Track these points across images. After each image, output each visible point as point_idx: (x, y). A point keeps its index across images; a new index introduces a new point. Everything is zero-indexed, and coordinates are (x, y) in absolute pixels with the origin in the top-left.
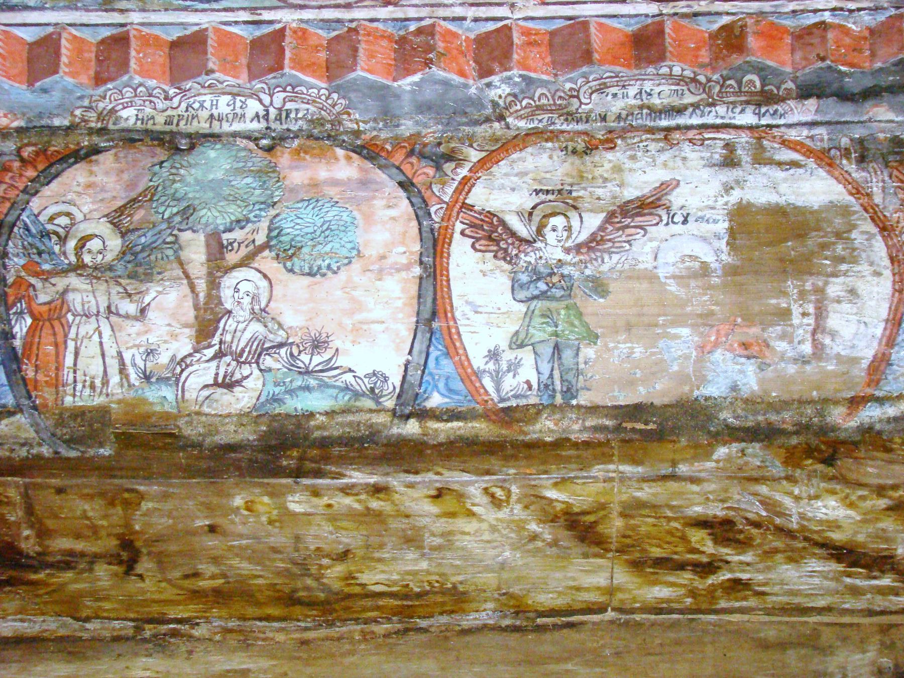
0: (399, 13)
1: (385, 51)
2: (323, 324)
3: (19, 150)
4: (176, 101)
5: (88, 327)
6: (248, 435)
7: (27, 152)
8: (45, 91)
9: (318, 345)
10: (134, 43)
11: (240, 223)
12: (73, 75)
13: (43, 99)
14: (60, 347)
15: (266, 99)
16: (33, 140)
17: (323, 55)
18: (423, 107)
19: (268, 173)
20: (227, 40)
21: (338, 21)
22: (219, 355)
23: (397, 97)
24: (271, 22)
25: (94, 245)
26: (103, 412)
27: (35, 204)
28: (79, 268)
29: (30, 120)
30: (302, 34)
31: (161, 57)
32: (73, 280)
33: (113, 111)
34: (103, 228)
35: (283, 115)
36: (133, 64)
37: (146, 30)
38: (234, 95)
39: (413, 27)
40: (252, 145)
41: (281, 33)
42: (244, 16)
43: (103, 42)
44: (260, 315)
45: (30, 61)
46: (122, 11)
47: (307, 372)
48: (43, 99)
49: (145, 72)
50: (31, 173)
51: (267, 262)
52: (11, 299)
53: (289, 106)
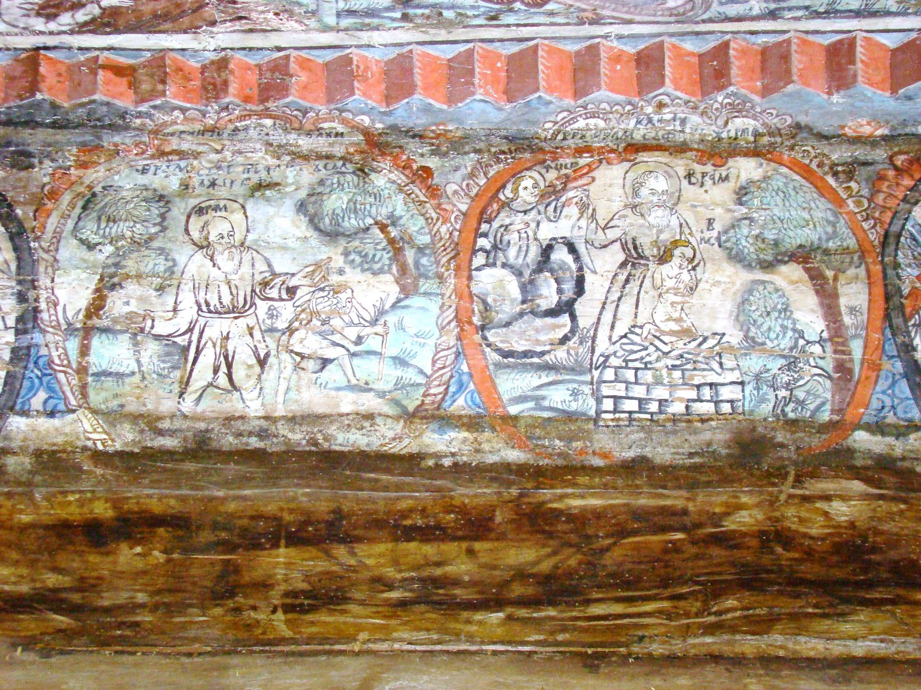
3: (891, 158)
7: (900, 160)
8: (909, 98)
13: (907, 106)
16: (904, 148)
29: (893, 128)
45: (893, 67)
50: (907, 182)
52: (908, 310)
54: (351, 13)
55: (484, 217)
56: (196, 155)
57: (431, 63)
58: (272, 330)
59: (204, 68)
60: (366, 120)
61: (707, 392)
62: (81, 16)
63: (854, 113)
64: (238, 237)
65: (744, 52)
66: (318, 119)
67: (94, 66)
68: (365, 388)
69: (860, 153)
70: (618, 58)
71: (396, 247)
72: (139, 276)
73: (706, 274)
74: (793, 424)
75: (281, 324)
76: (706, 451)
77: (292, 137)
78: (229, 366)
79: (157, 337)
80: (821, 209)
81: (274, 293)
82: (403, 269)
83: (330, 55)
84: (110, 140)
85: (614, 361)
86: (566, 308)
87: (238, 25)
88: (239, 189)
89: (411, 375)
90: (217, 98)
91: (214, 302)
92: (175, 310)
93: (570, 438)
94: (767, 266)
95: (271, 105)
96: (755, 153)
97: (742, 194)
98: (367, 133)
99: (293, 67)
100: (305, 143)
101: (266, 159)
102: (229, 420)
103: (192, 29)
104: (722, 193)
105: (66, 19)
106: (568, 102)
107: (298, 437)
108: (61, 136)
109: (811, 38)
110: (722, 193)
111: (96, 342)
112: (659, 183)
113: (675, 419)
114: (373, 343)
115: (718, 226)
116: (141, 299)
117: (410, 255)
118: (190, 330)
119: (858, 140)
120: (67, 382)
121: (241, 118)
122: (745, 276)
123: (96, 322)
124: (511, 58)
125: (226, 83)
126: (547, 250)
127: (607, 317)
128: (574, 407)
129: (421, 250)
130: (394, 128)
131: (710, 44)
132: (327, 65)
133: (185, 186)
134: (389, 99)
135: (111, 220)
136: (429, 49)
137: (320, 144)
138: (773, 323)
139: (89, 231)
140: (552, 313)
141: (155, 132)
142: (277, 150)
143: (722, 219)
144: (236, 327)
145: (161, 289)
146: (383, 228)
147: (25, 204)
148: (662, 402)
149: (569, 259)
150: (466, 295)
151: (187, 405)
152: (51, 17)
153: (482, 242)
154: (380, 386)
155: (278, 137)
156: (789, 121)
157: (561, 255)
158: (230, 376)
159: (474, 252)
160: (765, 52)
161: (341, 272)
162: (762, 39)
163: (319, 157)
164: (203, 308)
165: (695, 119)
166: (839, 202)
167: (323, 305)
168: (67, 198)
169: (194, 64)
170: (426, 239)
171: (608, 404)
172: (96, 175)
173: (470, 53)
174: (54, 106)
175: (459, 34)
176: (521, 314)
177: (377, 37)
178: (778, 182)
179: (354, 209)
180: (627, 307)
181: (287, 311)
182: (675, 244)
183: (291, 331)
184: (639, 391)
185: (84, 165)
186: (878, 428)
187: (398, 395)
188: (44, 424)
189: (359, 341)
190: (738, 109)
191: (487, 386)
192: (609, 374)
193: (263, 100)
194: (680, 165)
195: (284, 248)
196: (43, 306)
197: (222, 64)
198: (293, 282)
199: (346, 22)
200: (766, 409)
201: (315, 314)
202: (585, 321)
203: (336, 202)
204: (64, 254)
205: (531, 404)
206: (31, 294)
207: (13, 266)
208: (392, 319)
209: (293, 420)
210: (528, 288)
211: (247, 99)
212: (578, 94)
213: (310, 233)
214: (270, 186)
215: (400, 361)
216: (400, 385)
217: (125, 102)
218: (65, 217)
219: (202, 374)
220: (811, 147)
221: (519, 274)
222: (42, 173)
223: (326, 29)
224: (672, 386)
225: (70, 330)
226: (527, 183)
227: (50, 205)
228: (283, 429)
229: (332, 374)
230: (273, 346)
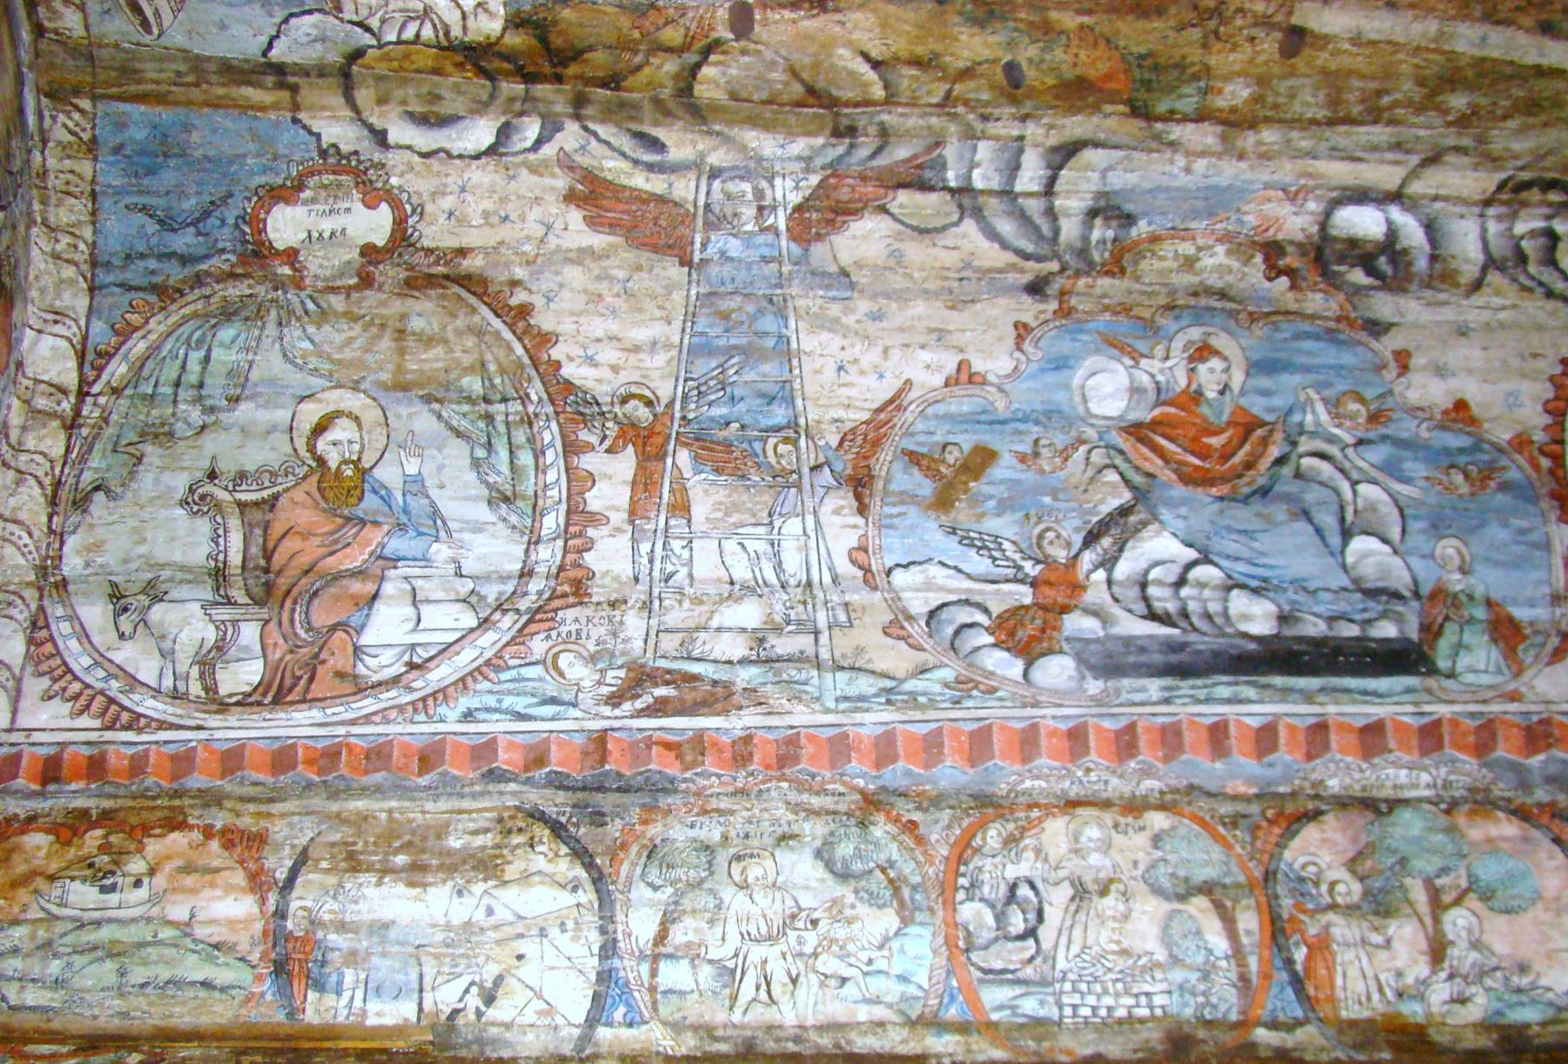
0: (1523, 708)
1: (1517, 737)
2: (1527, 951)
3: (1263, 812)
4: (1368, 773)
5: (1350, 955)
6: (1485, 1042)
7: (1270, 813)
8: (1271, 765)
9: (1523, 969)
10: (1332, 729)
11: (1444, 871)
12: (1290, 753)
14: (1331, 970)
15: (1434, 772)
17: (1471, 739)
18: (1550, 780)
19: (1451, 830)
20: (1400, 728)
21: (1481, 713)
22: (1451, 977)
23: (1530, 771)
24: (1430, 714)
25: (1340, 888)
26: (1370, 1022)
27: (1287, 855)
28: (1333, 907)
30: (1454, 723)
31: (1352, 739)
32: (1331, 917)
33: (1322, 781)
34: (1341, 874)
35: (1447, 784)
36: (1334, 745)
37: (1340, 719)
38: (1410, 769)
39: (1535, 718)
40: (1433, 808)
41: (1437, 723)
42: (1410, 709)
43: (1309, 728)
44: (1476, 945)
46: (1321, 704)
47: (1519, 990)
48: (1269, 772)
49: (1343, 751)
50: (1277, 831)
51: (1472, 901)
52: (1289, 931)
53: (1452, 777)
54: (846, 699)
55: (961, 860)
56: (732, 812)
57: (911, 738)
58: (801, 955)
59: (734, 743)
60: (861, 782)
61: (1143, 1000)
62: (639, 704)
63: (1232, 776)
64: (771, 879)
65: (1148, 730)
66: (823, 782)
67: (649, 743)
68: (876, 1001)
69: (1240, 807)
70: (1053, 733)
71: (895, 885)
72: (694, 911)
73: (1137, 906)
74: (1209, 1024)
75: (808, 949)
76: (1146, 1046)
77: (805, 797)
78: (768, 984)
79: (711, 962)
80: (1217, 852)
81: (800, 924)
82: (902, 904)
83: (831, 732)
84: (665, 801)
85: (1070, 976)
86: (1031, 933)
87: (759, 709)
88: (767, 840)
89: (912, 990)
90: (744, 766)
91: (754, 932)
92: (723, 939)
93: (1040, 1039)
94: (1182, 898)
95: (787, 771)
96: (1163, 807)
97: (1157, 840)
98: (862, 792)
99: (803, 741)
100: (816, 801)
101: (782, 812)
102: (769, 1028)
103: (725, 712)
104: (1141, 840)
105: (627, 706)
106: (1017, 767)
107: (825, 1041)
108: (626, 799)
109: (1197, 719)
110: (1141, 840)
111: (663, 966)
112: (1093, 832)
113: (1120, 1022)
114: (881, 964)
115: (1142, 867)
116: (697, 930)
117: (906, 892)
118: (736, 955)
119: (1235, 798)
120: (641, 998)
121: (763, 782)
122: (1166, 907)
123: (663, 950)
124: (972, 734)
125: (751, 754)
126: (1013, 888)
127: (1063, 940)
128: (1042, 1013)
129: (914, 888)
130: (884, 789)
131: (1122, 723)
132: (829, 739)
133: (725, 837)
134: (878, 765)
135: (670, 866)
136: (908, 727)
137: (827, 802)
138: (1189, 943)
139: (654, 875)
140: (1021, 937)
141: (698, 794)
142: (795, 808)
143: (1144, 860)
144: (772, 952)
145: (711, 922)
146: (883, 870)
147: (603, 854)
148: (1109, 1009)
149: (1031, 894)
150: (952, 924)
151: (736, 1017)
152: (616, 705)
153: (962, 881)
154: (889, 999)
155: (793, 797)
156: (1185, 782)
157: (1024, 891)
158: (769, 992)
159: (956, 889)
160: (1164, 730)
161: (853, 906)
162: (1161, 720)
163: (828, 813)
164: (745, 936)
165: (1115, 781)
166: (1228, 846)
167: (841, 932)
168: (634, 849)
169: (726, 739)
170: (916, 879)
171: (1068, 1011)
172: (655, 830)
173: (939, 731)
174: (619, 775)
175: (931, 715)
176: (996, 939)
177: (868, 718)
178: (1183, 831)
179: (858, 854)
180: (1077, 933)
181: (811, 939)
182: (1111, 881)
183: (815, 955)
184: (1091, 1000)
185: (645, 822)
186: (1274, 1025)
187: (903, 1006)
188: (625, 1033)
189: (870, 962)
190: (1146, 772)
191: (973, 1001)
192: (1068, 986)
193: (780, 768)
194: (1108, 817)
195: (807, 888)
196: (620, 936)
197: (747, 739)
198: (815, 915)
199: (843, 706)
200: (1188, 1012)
201: (833, 941)
202: (1046, 945)
203: (845, 849)
204: (634, 895)
205: (1007, 1012)
206: (611, 928)
207: (596, 906)
208: (895, 944)
209: (821, 1028)
210: (1000, 918)
211: (768, 767)
212: (1025, 760)
213: (827, 875)
214: (793, 837)
215: (903, 978)
216: (904, 998)
217: (673, 771)
218: (634, 864)
219: (747, 991)
220: (1202, 805)
221: (992, 906)
222: (614, 829)
223: (827, 711)
224: (1117, 995)
225: (642, 957)
226: (992, 832)
227: (622, 855)
228: (813, 1036)
229: (850, 990)
230: (802, 967)
